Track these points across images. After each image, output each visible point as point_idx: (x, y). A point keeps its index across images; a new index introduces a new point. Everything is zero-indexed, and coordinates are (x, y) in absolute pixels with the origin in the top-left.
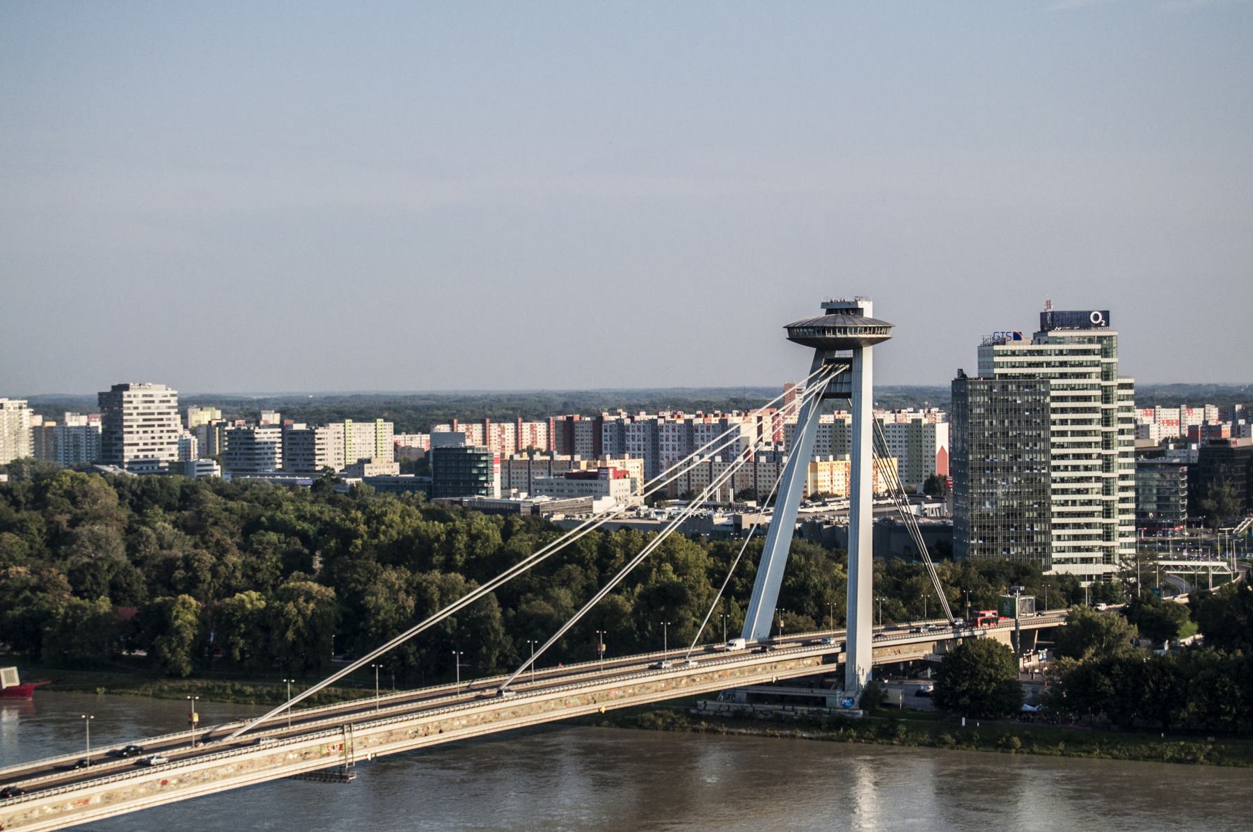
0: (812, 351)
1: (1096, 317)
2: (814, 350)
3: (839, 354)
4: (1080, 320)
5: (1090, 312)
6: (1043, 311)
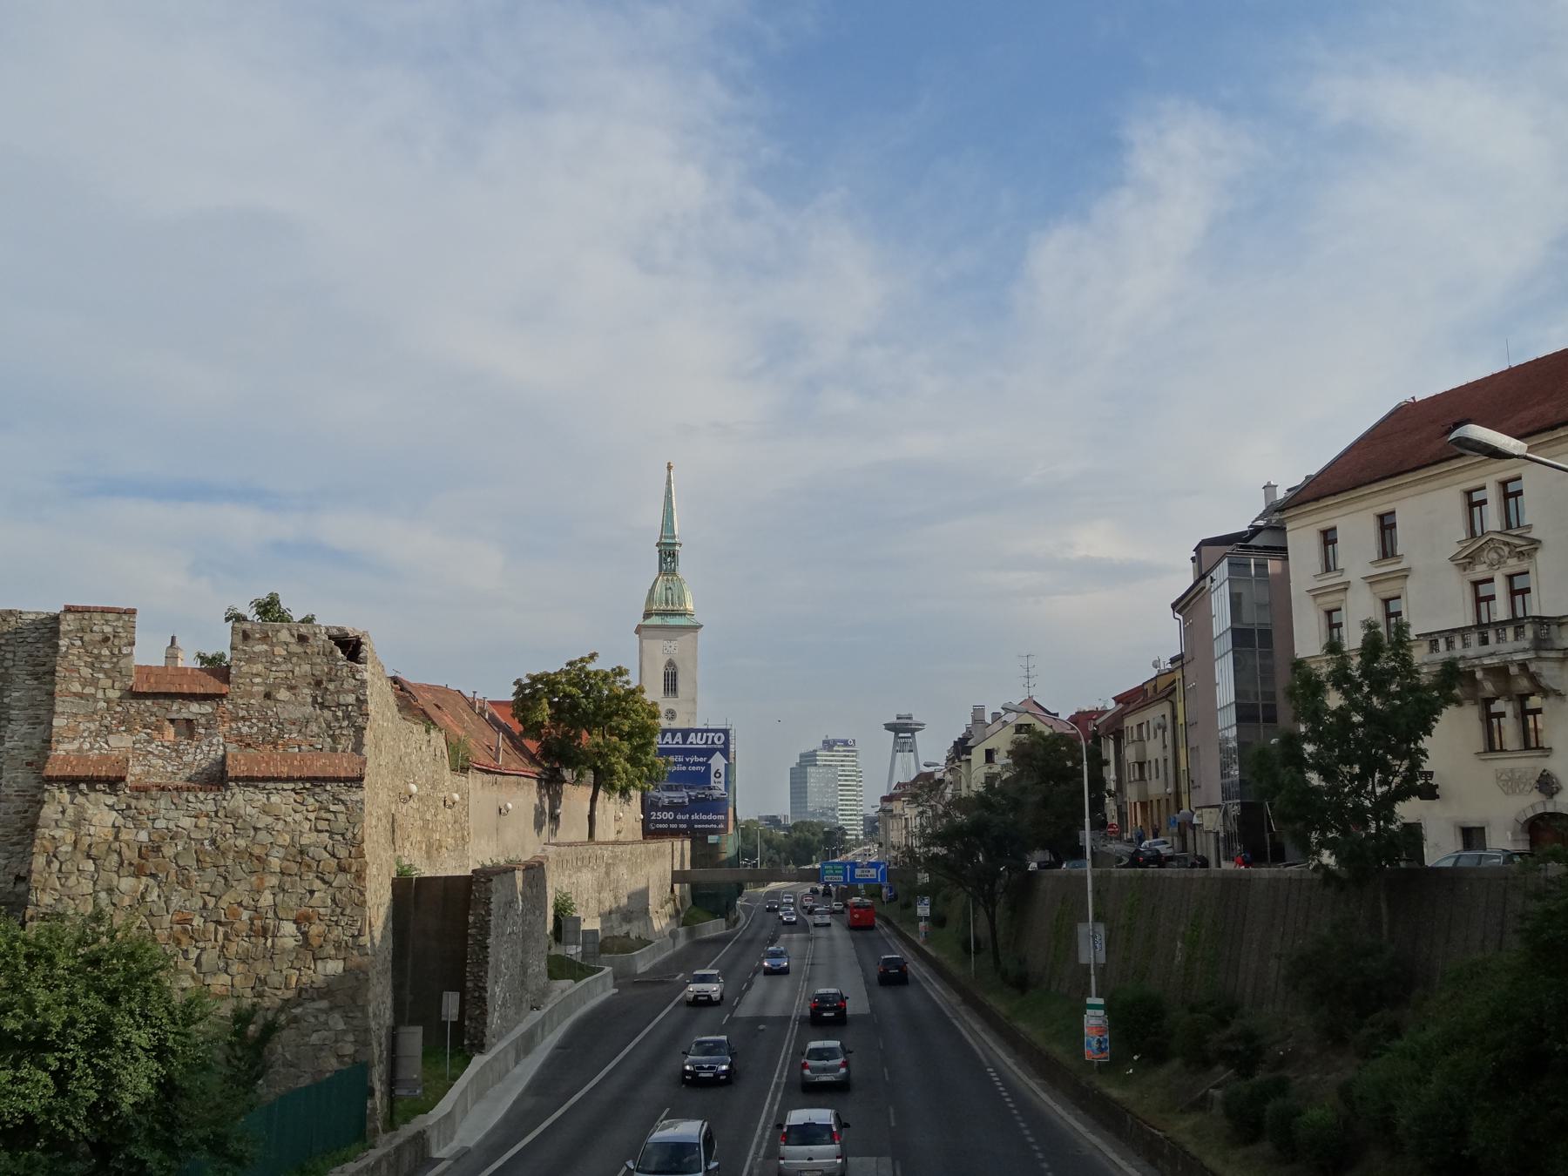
3: (901, 735)
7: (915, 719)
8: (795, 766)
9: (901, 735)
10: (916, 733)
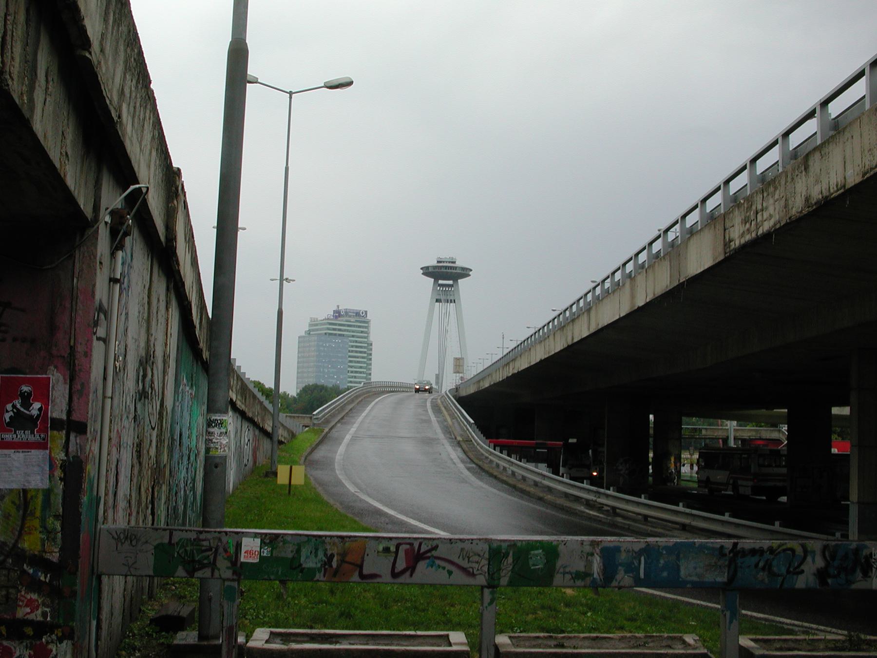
1: (363, 313)
2: (433, 280)
4: (357, 314)
7: (459, 263)
8: (303, 334)
9: (441, 282)
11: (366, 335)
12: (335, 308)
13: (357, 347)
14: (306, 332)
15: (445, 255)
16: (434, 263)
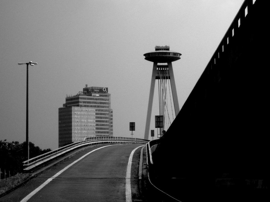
0: (152, 63)
4: (101, 91)
5: (103, 89)
6: (84, 88)
7: (172, 50)
8: (62, 106)
9: (159, 64)
10: (173, 63)
11: (108, 105)
12: (84, 87)
13: (101, 114)
14: (64, 105)
15: (162, 44)
16: (153, 50)
